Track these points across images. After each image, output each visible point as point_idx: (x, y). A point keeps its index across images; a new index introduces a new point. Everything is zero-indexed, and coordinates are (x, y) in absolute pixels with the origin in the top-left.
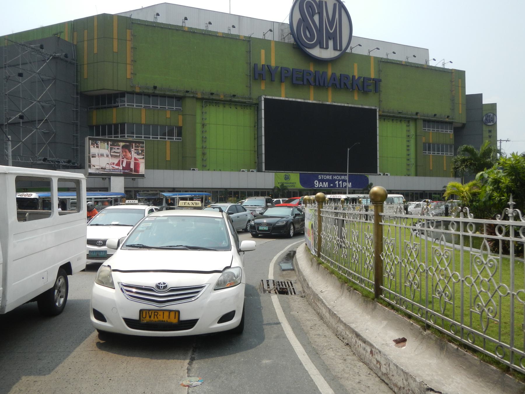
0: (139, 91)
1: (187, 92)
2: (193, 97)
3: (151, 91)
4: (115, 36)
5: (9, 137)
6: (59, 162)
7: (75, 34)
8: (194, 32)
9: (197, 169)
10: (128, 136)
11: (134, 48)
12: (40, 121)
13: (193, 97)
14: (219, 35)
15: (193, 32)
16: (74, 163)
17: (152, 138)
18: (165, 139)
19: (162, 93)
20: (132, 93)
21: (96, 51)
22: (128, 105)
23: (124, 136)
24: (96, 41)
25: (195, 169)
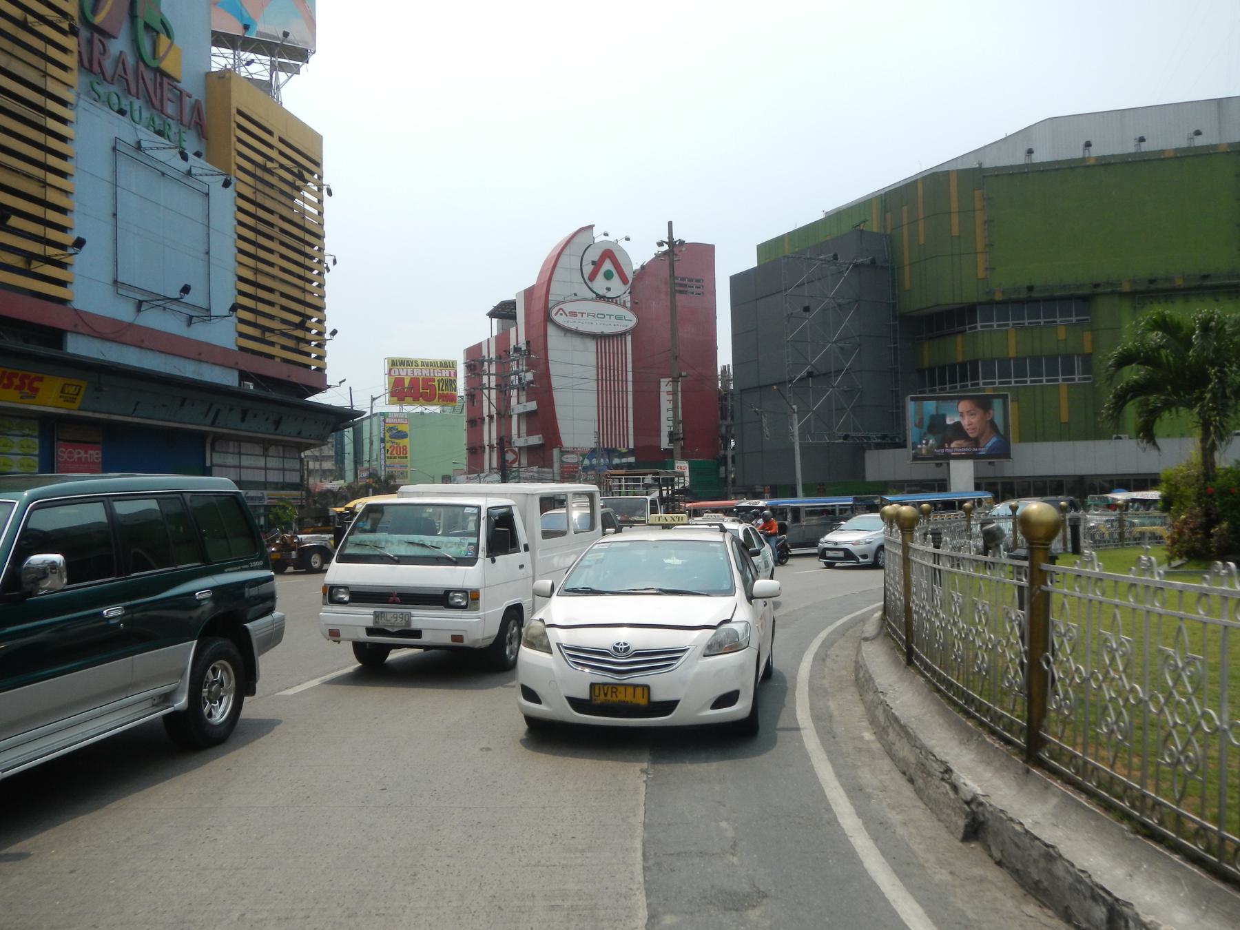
0: (1001, 299)
1: (1097, 286)
2: (1113, 293)
3: (1024, 295)
4: (954, 206)
5: (794, 406)
6: (868, 438)
7: (889, 215)
8: (1109, 164)
9: (1127, 436)
10: (984, 384)
11: (989, 222)
12: (838, 372)
13: (1113, 293)
14: (1167, 155)
15: (1107, 163)
16: (893, 439)
17: (1031, 382)
18: (1057, 380)
19: (1047, 294)
20: (991, 303)
21: (922, 240)
22: (982, 327)
23: (978, 384)
24: (921, 224)
25: (1122, 436)
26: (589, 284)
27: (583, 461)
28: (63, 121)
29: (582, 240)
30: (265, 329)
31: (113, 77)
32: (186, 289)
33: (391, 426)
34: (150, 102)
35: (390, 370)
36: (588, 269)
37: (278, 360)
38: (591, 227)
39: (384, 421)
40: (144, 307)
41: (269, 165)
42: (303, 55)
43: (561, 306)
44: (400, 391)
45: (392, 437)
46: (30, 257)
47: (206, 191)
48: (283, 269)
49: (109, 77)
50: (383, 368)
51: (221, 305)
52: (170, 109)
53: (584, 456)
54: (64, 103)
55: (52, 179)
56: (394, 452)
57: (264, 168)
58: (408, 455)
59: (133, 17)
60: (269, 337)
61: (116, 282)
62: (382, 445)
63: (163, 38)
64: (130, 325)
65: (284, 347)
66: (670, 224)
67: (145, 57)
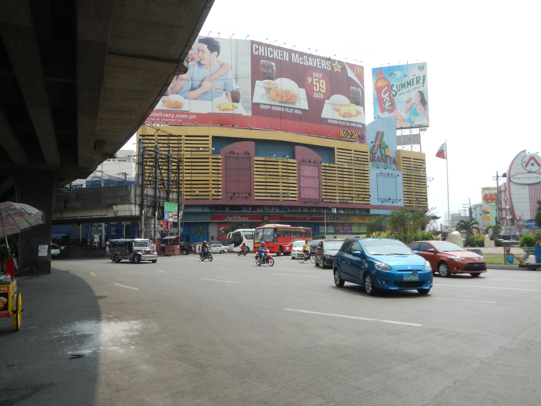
26: (525, 168)
27: (525, 224)
28: (368, 174)
29: (523, 155)
30: (410, 201)
31: (377, 160)
32: (390, 199)
33: (483, 210)
34: (384, 162)
35: (482, 192)
36: (524, 165)
37: (414, 206)
38: (525, 150)
39: (481, 208)
40: (383, 202)
41: (410, 166)
42: (428, 126)
43: (514, 177)
44: (486, 198)
45: (484, 213)
46: (364, 198)
47: (395, 176)
48: (415, 187)
49: (376, 161)
50: (480, 191)
51: (398, 200)
52: (388, 162)
53: (525, 222)
54: (367, 171)
55: (367, 184)
56: (485, 218)
57: (409, 167)
58: (490, 219)
59: (380, 148)
60: (411, 202)
61: (378, 198)
62: (481, 216)
63: (386, 149)
64: (381, 206)
65: (416, 204)
66: (497, 172)
67: (383, 154)
